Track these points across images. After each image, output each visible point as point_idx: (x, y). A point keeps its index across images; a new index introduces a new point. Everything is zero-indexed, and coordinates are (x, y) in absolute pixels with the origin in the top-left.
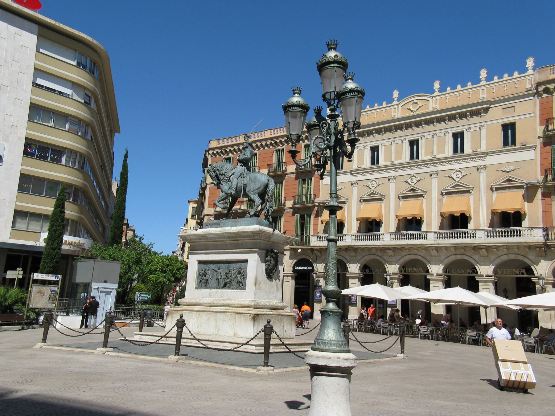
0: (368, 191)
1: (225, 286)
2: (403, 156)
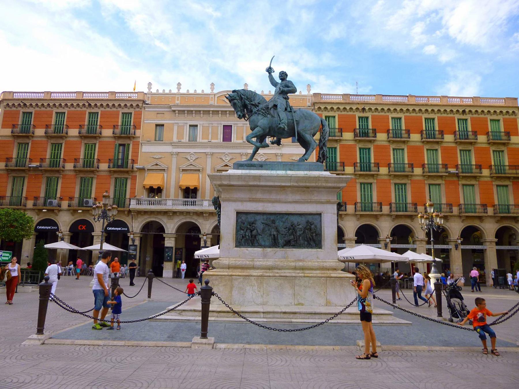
0: (188, 163)
1: (288, 244)
2: (219, 137)
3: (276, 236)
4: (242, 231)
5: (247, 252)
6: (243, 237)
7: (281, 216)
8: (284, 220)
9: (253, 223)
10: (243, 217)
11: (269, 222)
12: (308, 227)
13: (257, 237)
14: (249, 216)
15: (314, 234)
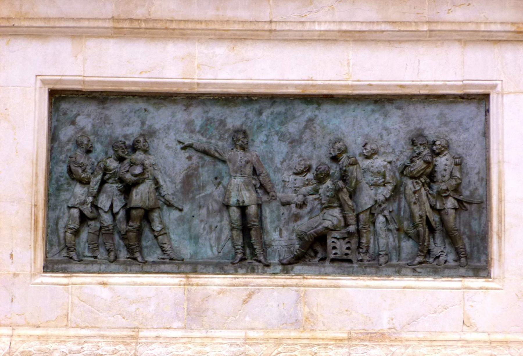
1: (312, 252)
3: (252, 210)
4: (79, 190)
5: (104, 293)
6: (83, 219)
7: (280, 108)
8: (293, 128)
9: (134, 149)
10: (86, 117)
11: (220, 144)
12: (419, 164)
13: (155, 215)
14: (115, 112)
15: (450, 203)
